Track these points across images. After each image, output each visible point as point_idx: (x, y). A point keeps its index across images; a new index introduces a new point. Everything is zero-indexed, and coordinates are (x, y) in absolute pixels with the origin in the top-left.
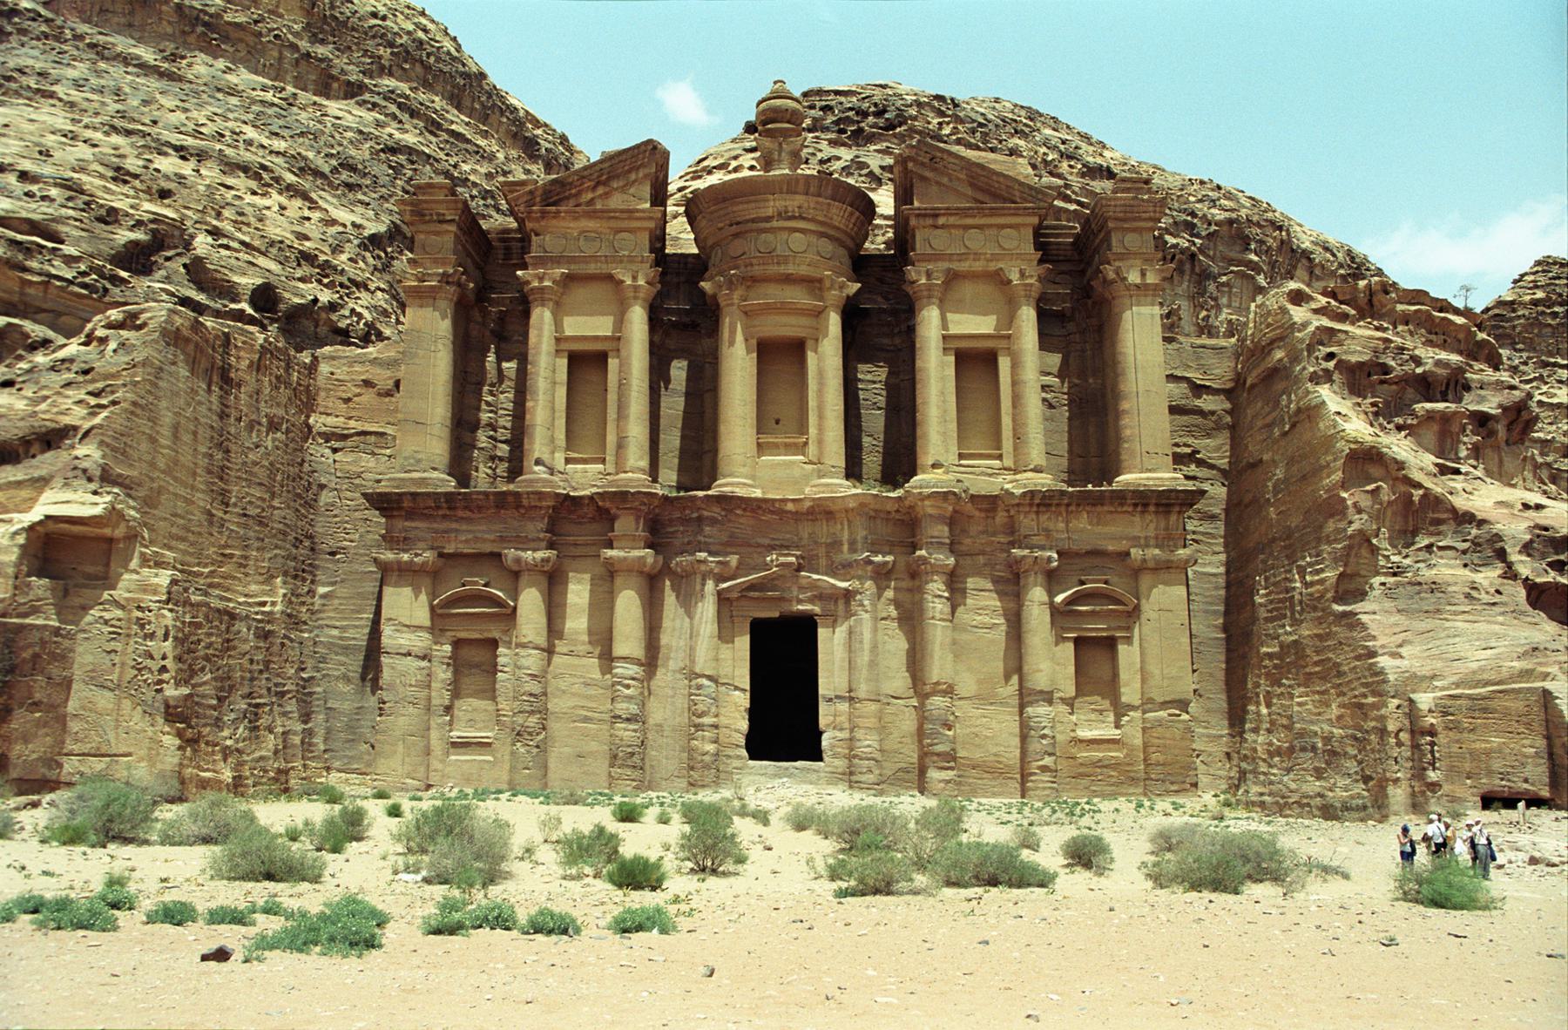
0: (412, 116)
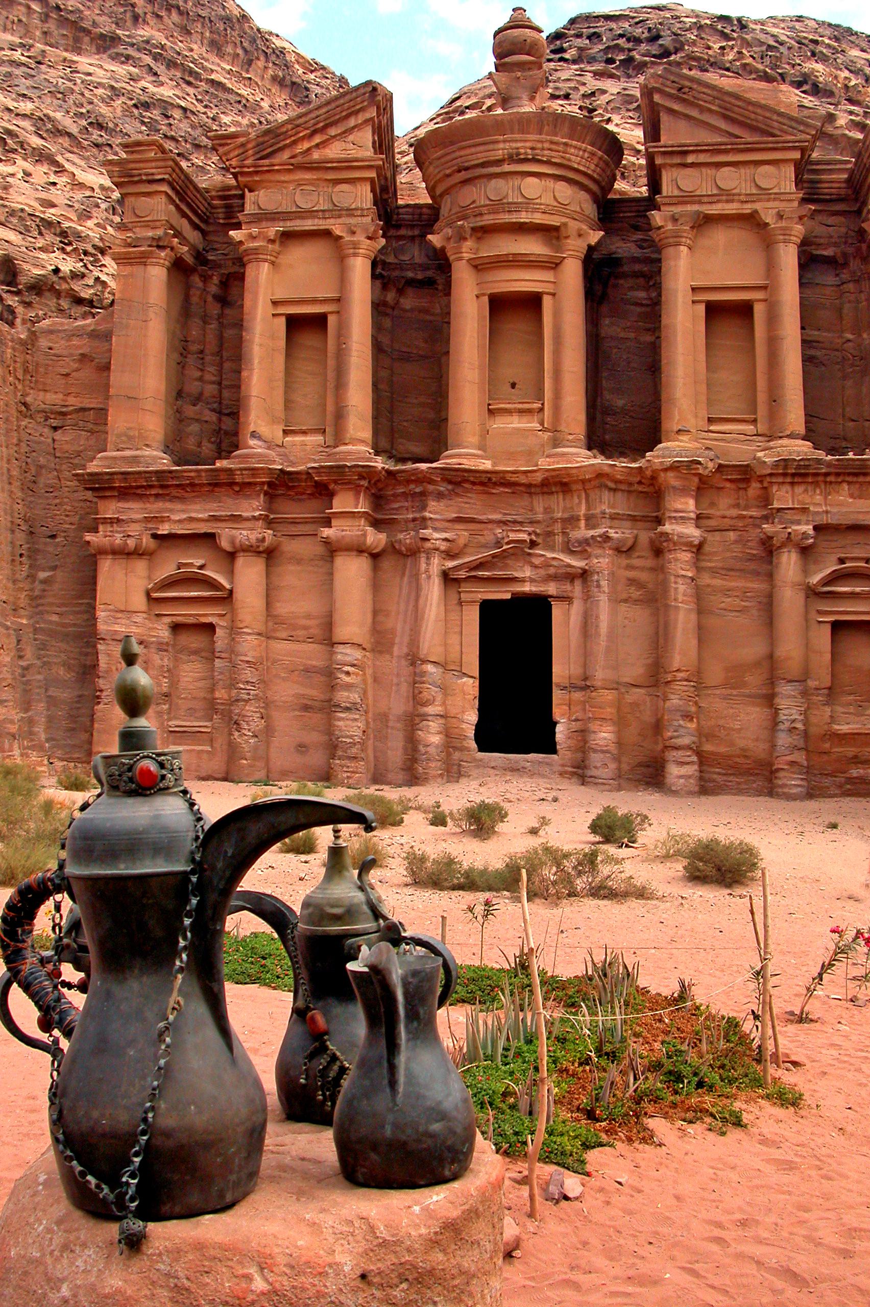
0: (168, 67)
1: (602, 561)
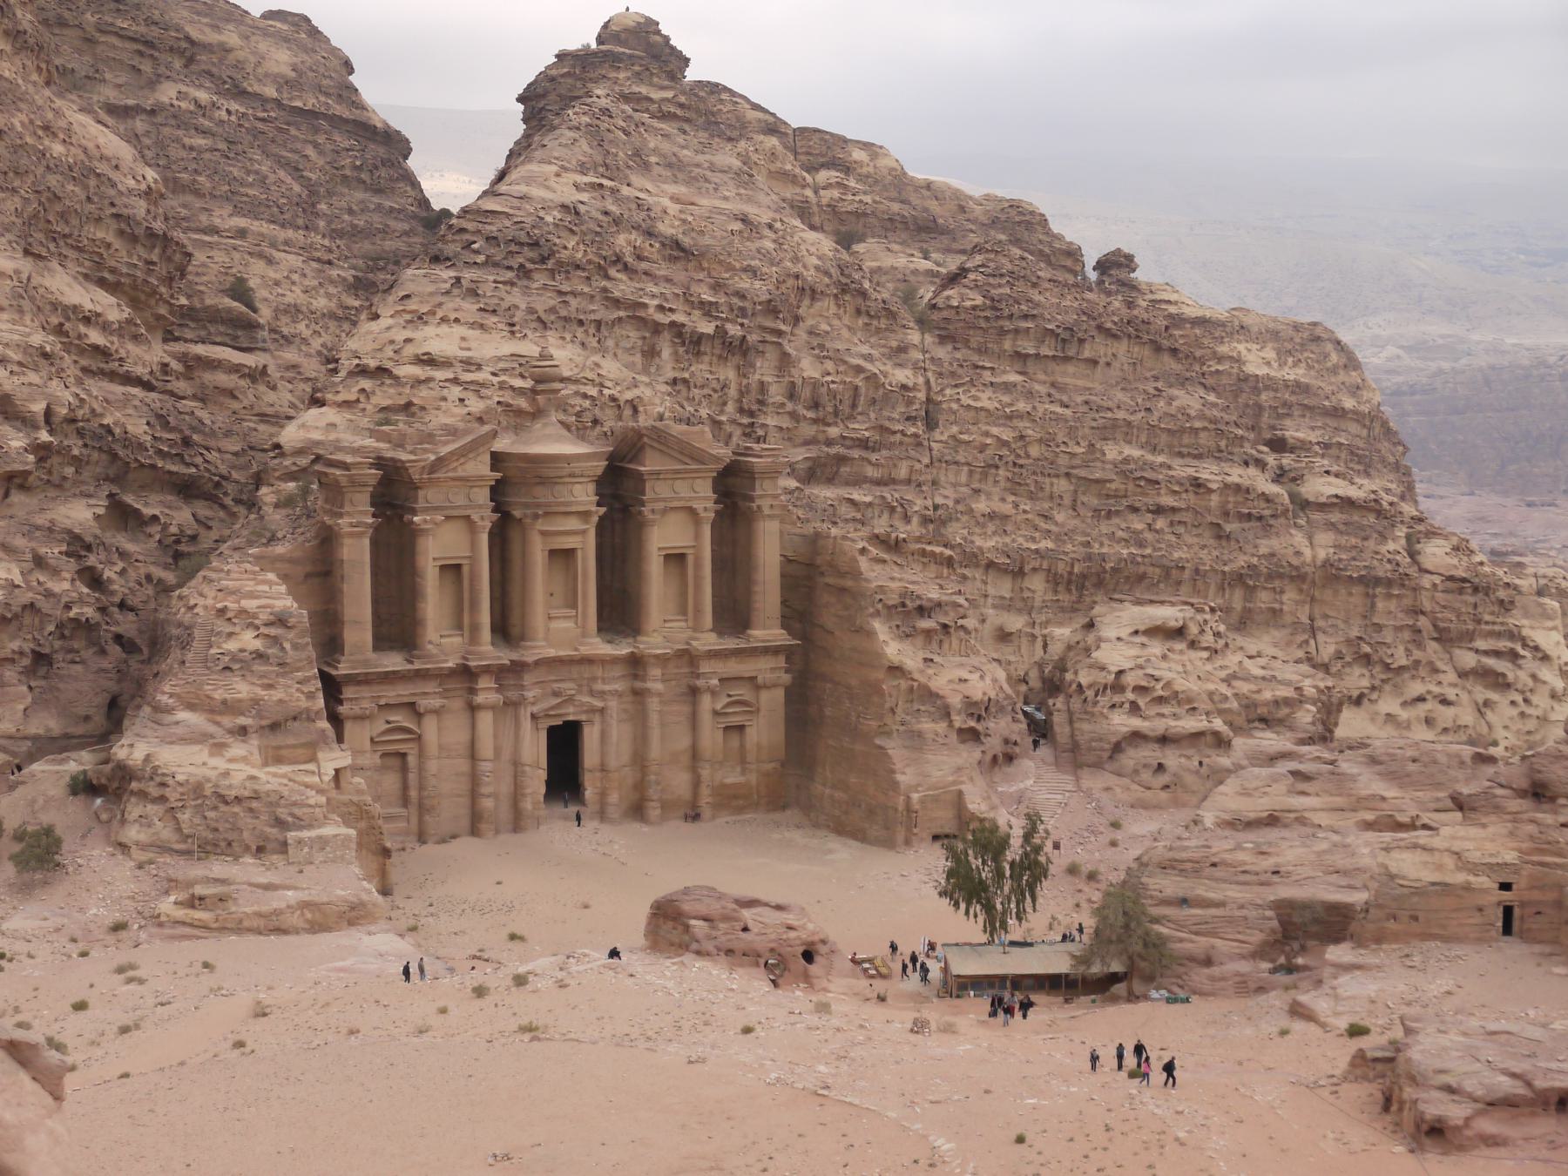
1: (613, 704)
